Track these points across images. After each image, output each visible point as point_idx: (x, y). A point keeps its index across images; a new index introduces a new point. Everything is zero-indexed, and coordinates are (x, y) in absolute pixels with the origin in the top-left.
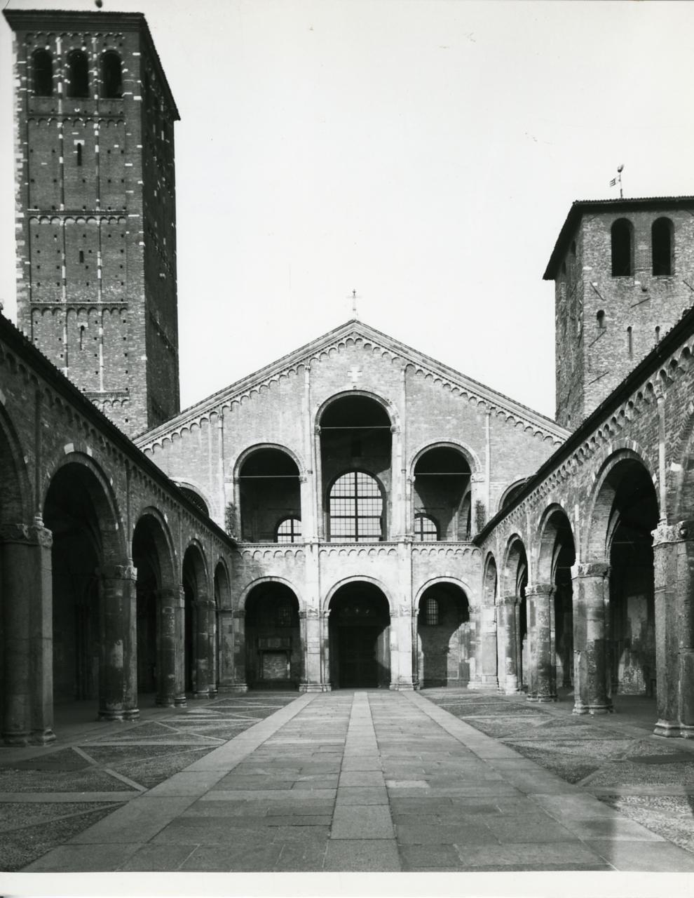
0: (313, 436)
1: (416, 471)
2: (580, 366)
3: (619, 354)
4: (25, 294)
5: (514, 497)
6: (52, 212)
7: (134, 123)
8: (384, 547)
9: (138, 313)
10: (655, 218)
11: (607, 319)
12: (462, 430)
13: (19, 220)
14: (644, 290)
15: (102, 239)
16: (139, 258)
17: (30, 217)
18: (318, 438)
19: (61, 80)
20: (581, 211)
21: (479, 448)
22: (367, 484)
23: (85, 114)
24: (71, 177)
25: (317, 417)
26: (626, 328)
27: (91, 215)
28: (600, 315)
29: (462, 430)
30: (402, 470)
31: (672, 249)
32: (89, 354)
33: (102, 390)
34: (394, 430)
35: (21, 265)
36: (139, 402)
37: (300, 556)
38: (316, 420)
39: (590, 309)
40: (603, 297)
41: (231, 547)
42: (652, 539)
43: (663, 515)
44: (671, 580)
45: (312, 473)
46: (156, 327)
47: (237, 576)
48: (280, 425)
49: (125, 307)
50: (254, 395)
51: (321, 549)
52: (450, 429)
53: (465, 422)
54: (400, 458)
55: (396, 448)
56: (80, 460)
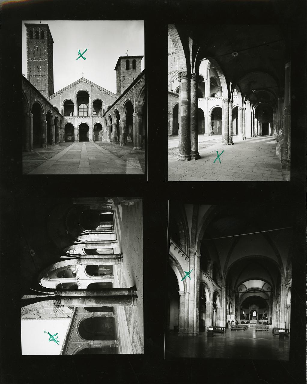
2: (121, 85)
4: (28, 73)
5: (110, 108)
6: (33, 59)
7: (46, 43)
9: (47, 76)
13: (27, 60)
15: (41, 63)
16: (47, 67)
17: (29, 60)
19: (34, 36)
20: (121, 58)
21: (104, 99)
22: (85, 106)
23: (38, 42)
24: (36, 53)
27: (39, 59)
32: (39, 84)
33: (41, 90)
35: (28, 68)
36: (47, 92)
41: (62, 117)
42: (133, 115)
43: (134, 111)
44: (136, 122)
46: (50, 79)
47: (63, 122)
49: (45, 75)
50: (66, 91)
56: (37, 102)
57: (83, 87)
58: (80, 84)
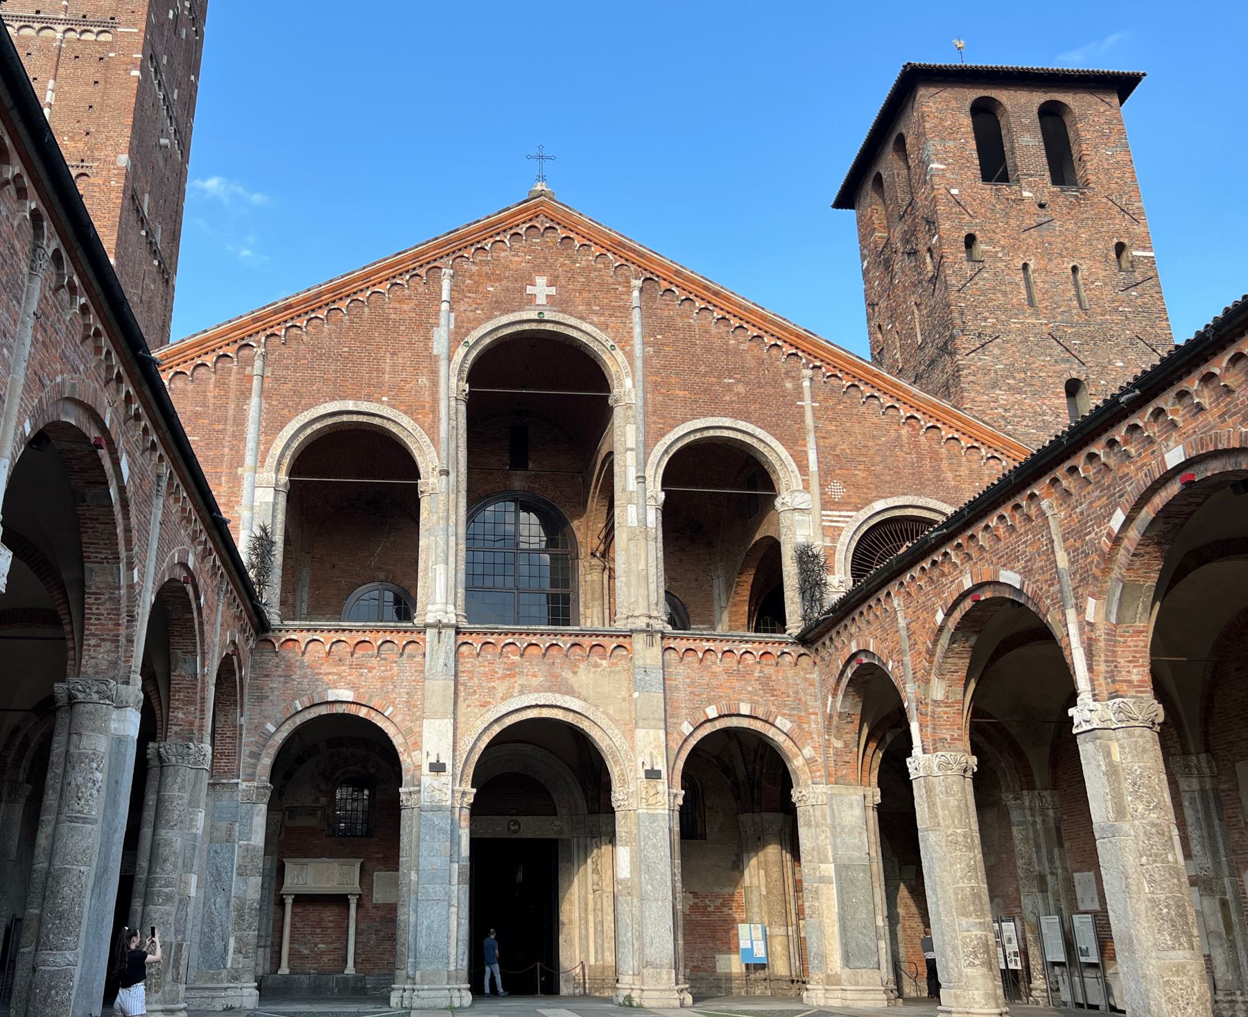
0: (453, 403)
1: (665, 483)
3: (1013, 306)
8: (600, 640)
10: (1042, 101)
11: (983, 247)
12: (758, 406)
14: (1042, 206)
18: (463, 408)
21: (793, 442)
25: (461, 366)
26: (1020, 266)
28: (970, 240)
29: (758, 406)
30: (637, 477)
31: (1074, 149)
34: (616, 401)
37: (411, 656)
38: (461, 371)
39: (950, 230)
40: (971, 212)
45: (447, 473)
48: (387, 376)
51: (462, 638)
52: (732, 402)
53: (762, 390)
54: (634, 453)
55: (624, 434)
57: (541, 289)
58: (512, 256)
